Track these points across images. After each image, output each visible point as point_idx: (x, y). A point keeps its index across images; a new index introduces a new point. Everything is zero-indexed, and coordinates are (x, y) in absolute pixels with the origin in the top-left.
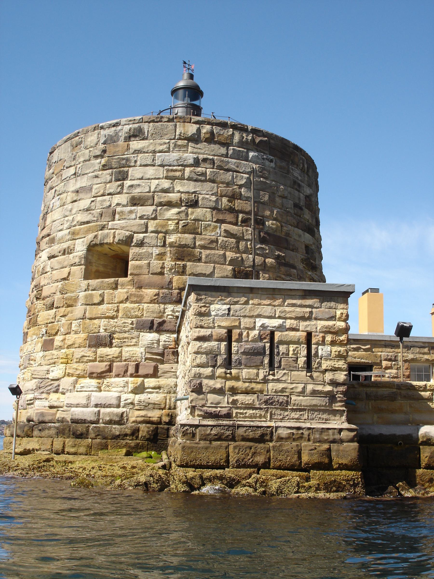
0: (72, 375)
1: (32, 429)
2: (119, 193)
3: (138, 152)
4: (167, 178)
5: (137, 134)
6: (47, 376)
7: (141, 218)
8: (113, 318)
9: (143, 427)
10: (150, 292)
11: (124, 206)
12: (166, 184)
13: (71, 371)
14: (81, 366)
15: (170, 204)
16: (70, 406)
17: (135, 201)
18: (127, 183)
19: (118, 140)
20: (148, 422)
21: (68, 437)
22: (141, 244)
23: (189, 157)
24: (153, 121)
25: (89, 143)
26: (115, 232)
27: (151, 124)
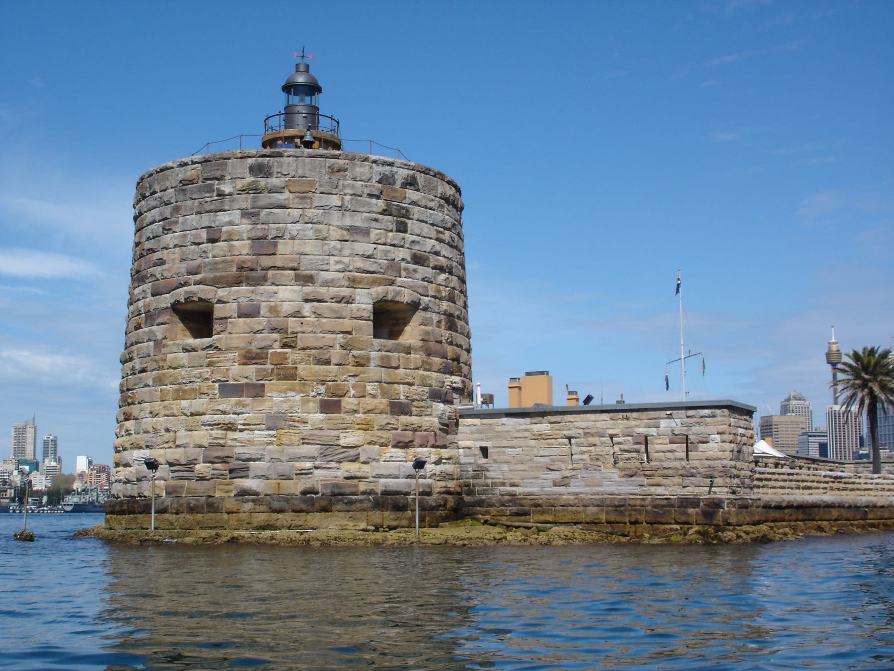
0: (375, 443)
1: (331, 503)
2: (402, 247)
3: (414, 203)
4: (437, 239)
5: (410, 183)
6: (337, 442)
7: (423, 280)
8: (410, 384)
9: (449, 497)
10: (437, 360)
11: (408, 262)
13: (375, 439)
14: (386, 435)
15: (440, 269)
16: (379, 476)
17: (418, 260)
18: (409, 237)
19: (394, 183)
20: (448, 493)
21: (387, 510)
22: (426, 309)
24: (424, 172)
25: (358, 175)
27: (422, 175)
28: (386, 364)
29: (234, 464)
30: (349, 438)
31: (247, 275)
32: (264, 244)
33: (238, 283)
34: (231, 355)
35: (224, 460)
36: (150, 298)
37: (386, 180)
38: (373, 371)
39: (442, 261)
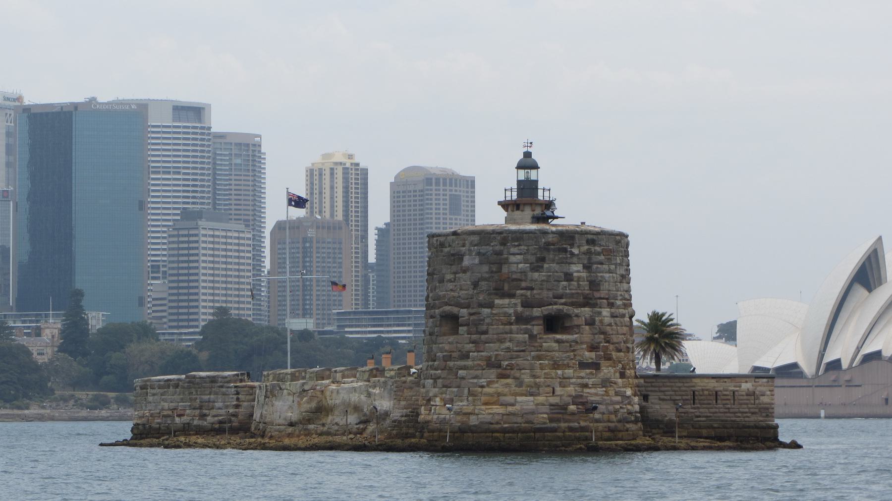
29: (589, 406)
31: (588, 302)
32: (594, 285)
33: (584, 306)
34: (585, 346)
35: (583, 404)
36: (520, 309)
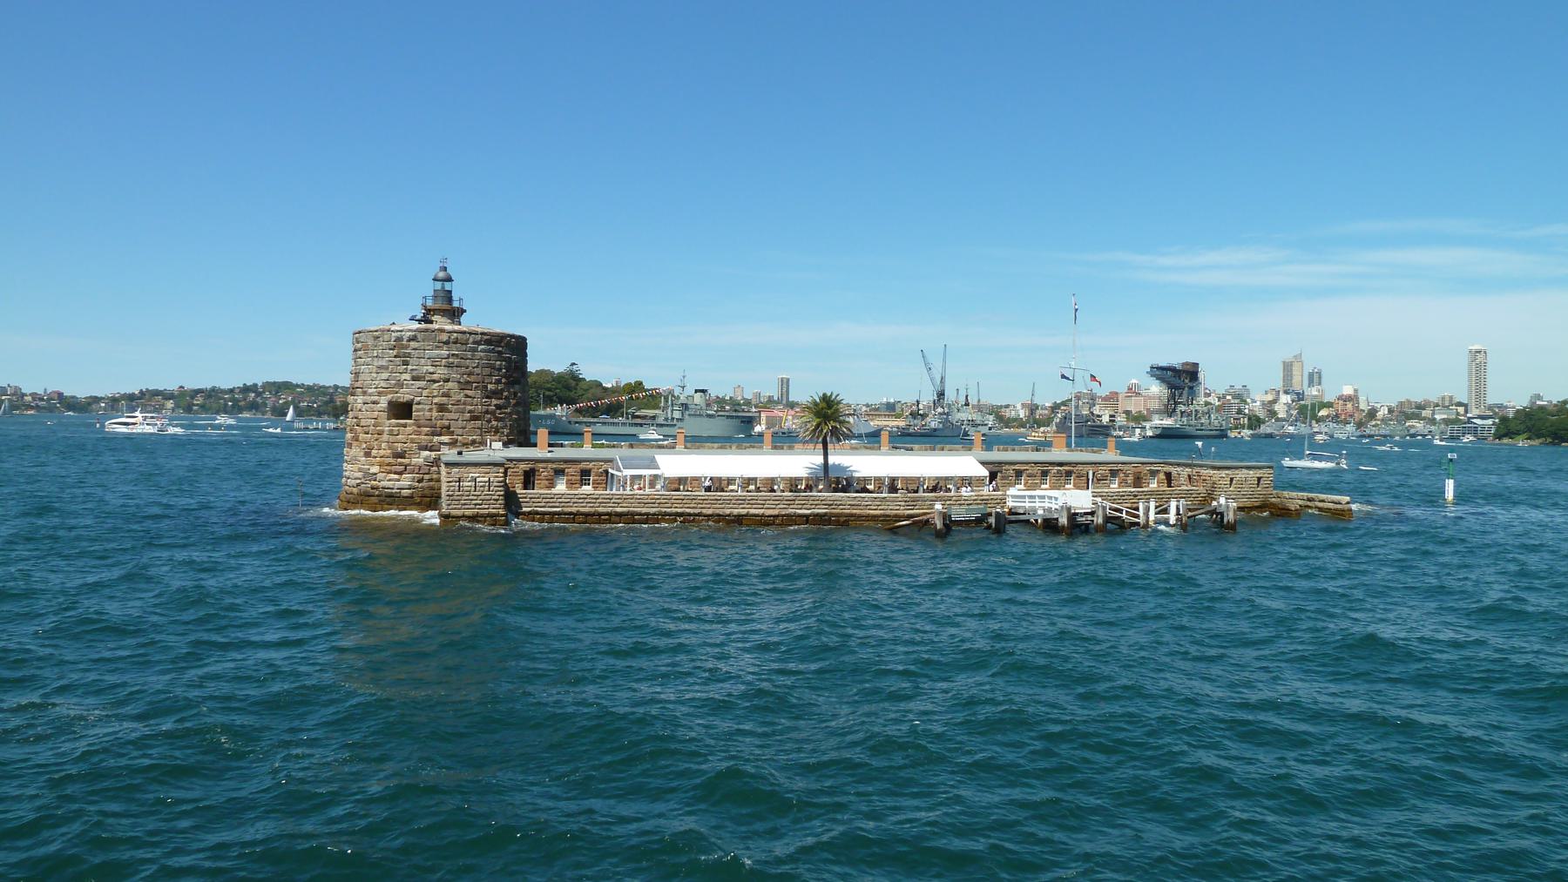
12: (431, 369)
17: (414, 379)
23: (445, 353)
26: (404, 396)
28: (391, 433)
30: (375, 469)
37: (399, 339)
38: (385, 437)
39: (435, 377)
